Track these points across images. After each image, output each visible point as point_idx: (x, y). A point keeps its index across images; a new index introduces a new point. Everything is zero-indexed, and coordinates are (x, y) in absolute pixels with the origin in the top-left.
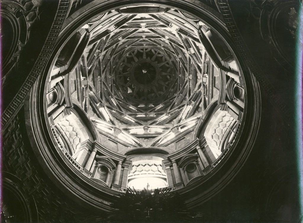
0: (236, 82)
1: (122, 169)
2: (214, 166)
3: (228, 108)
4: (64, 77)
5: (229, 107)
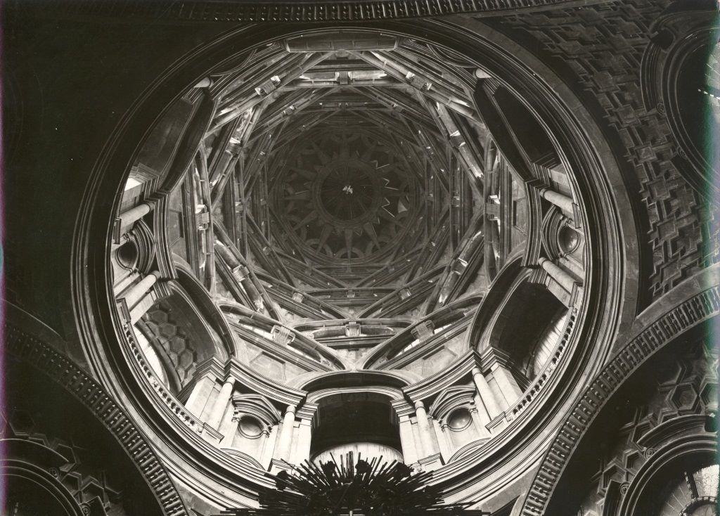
1: (297, 424)
3: (548, 278)
4: (153, 206)
5: (548, 275)
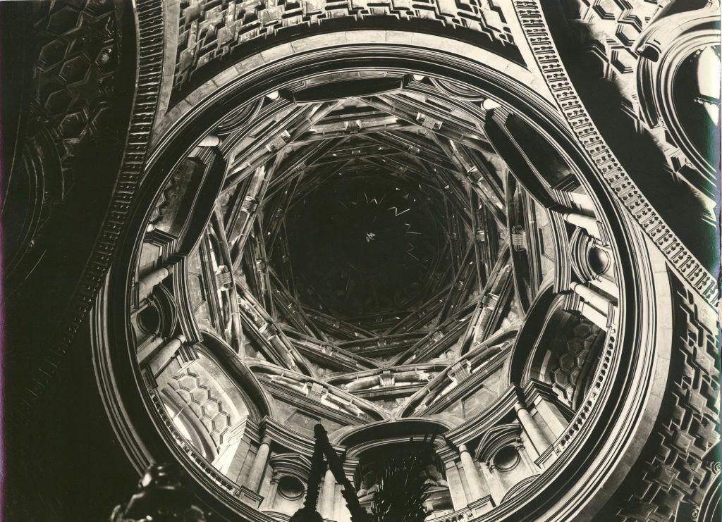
0: (591, 237)
2: (562, 449)
3: (581, 303)
5: (582, 299)
